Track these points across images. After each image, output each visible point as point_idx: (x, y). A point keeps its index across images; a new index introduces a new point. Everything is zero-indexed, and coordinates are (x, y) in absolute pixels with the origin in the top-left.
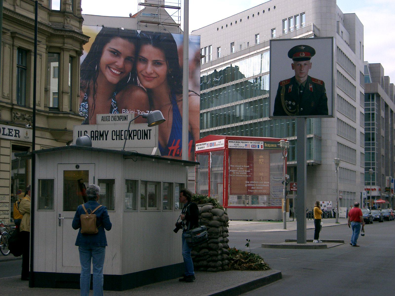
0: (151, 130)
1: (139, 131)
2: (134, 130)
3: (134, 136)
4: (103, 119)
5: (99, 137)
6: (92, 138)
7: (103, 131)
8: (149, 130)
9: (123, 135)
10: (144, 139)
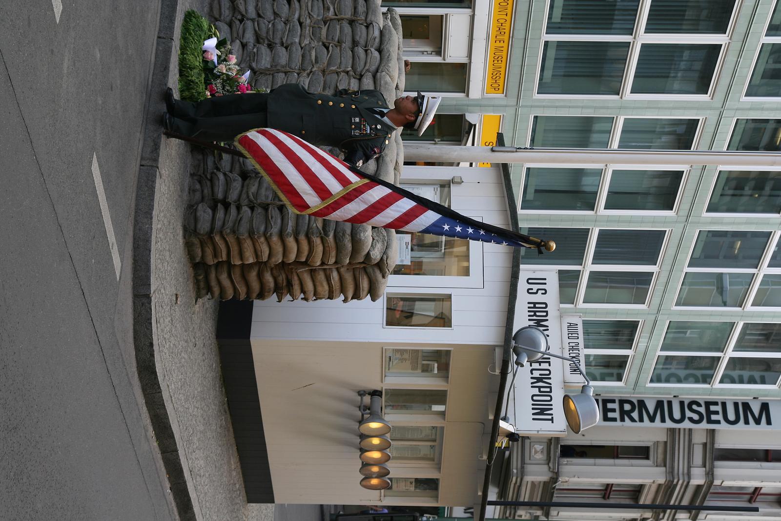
0: (553, 422)
1: (549, 398)
2: (550, 388)
3: (539, 387)
4: (570, 325)
5: (535, 318)
6: (532, 305)
7: (548, 327)
8: (552, 417)
9: (540, 365)
10: (533, 409)
